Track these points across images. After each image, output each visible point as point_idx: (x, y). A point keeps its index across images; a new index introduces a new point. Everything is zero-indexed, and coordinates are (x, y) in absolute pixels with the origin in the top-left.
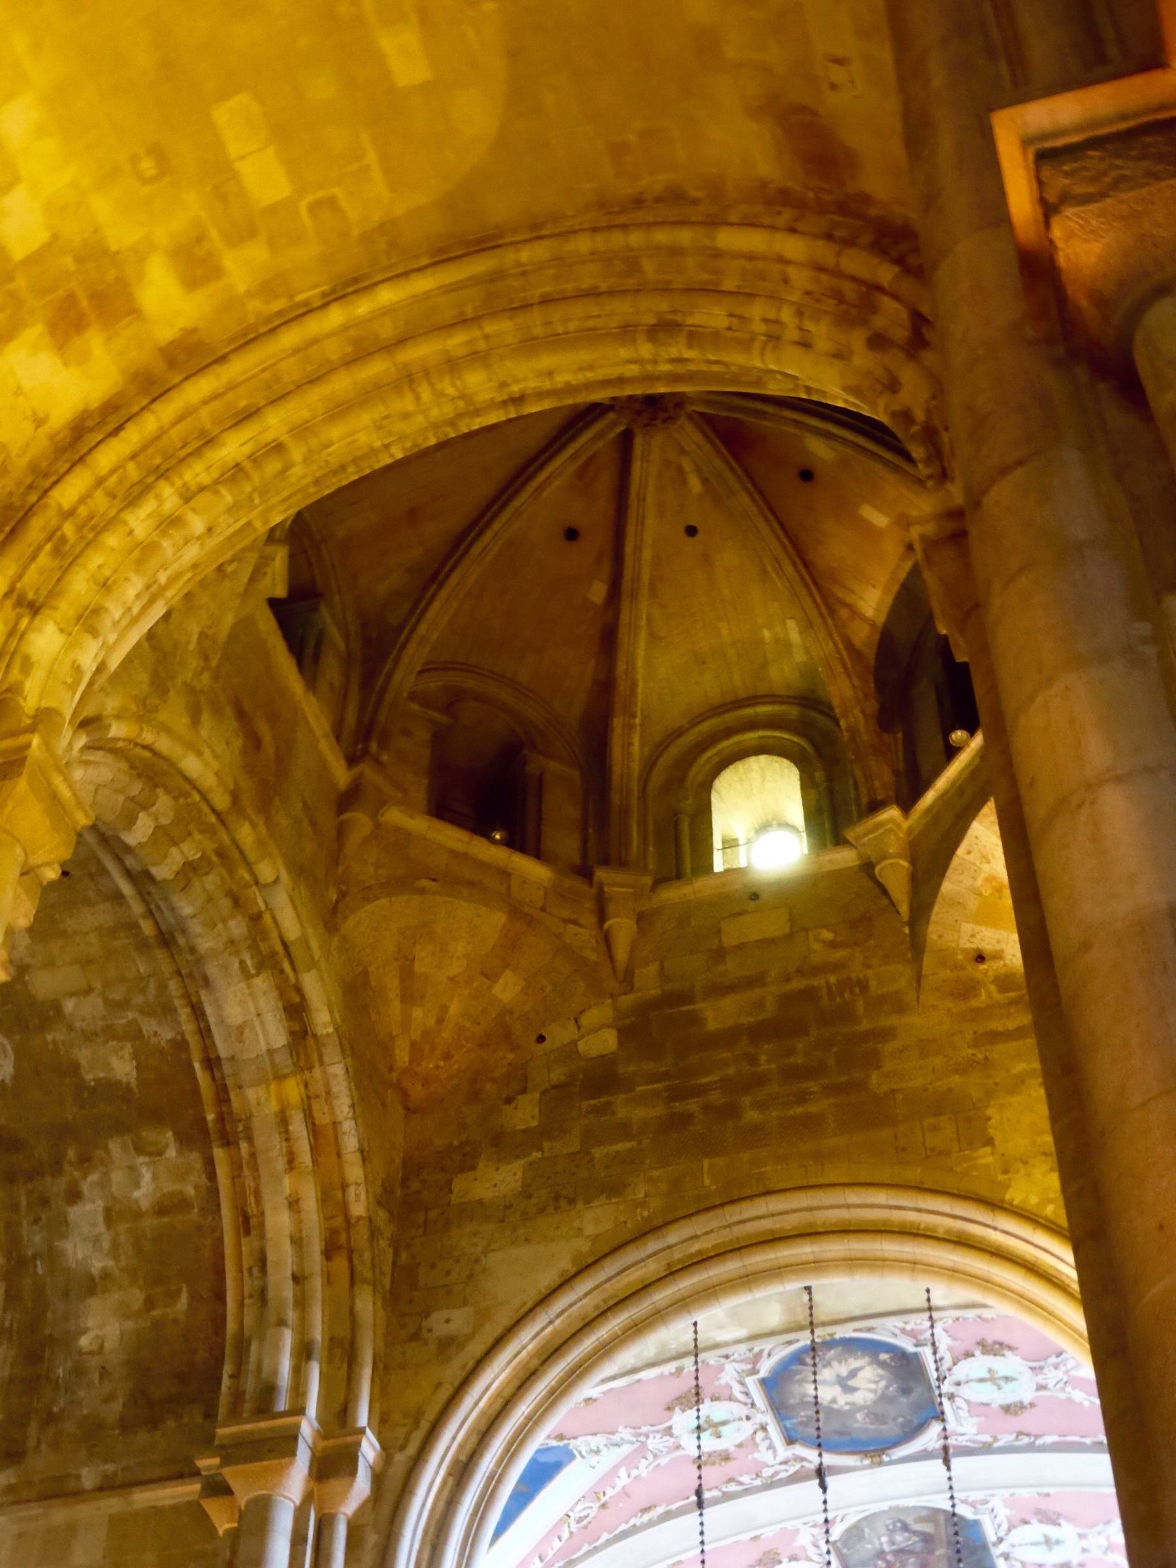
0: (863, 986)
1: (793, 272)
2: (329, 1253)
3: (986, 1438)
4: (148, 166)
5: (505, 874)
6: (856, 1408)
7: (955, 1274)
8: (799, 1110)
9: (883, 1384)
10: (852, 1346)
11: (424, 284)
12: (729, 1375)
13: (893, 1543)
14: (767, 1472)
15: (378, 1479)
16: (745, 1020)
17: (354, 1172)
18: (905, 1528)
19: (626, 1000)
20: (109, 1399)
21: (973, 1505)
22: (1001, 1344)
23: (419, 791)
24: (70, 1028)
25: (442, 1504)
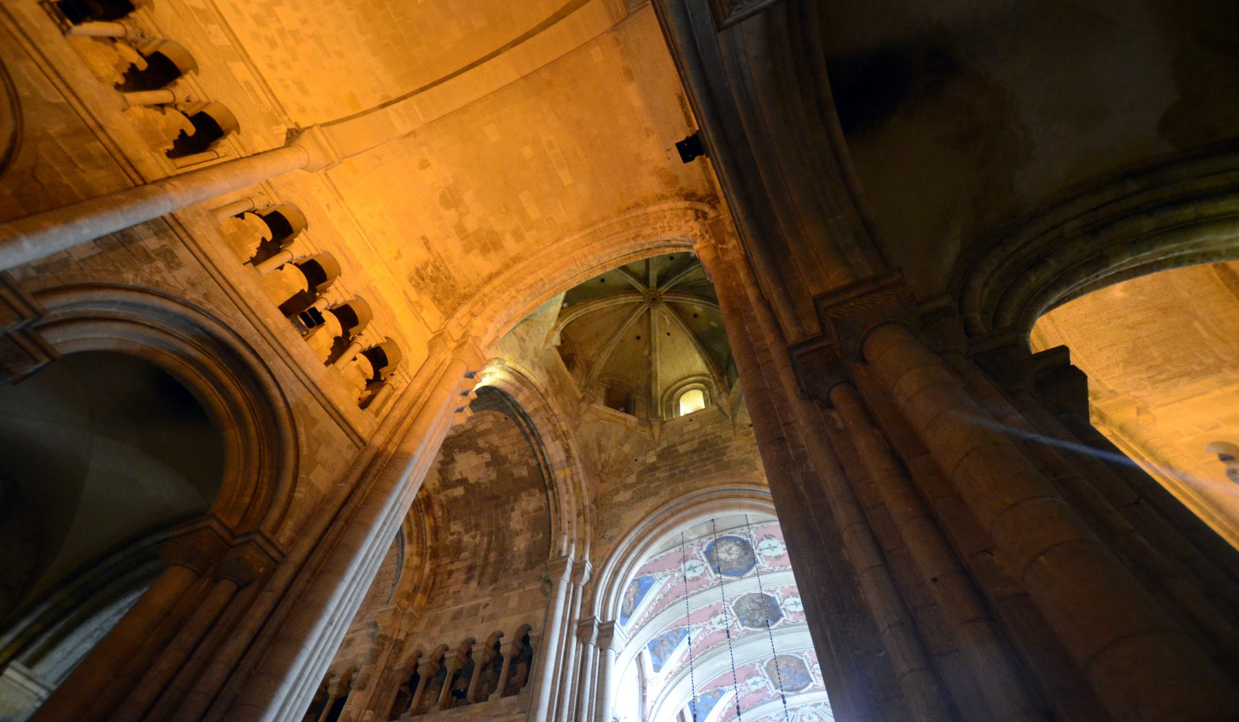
0: (720, 437)
1: (666, 213)
2: (578, 516)
3: (772, 568)
4: (503, 210)
5: (625, 419)
6: (733, 560)
7: (752, 507)
8: (704, 468)
9: (739, 551)
10: (728, 539)
11: (576, 236)
12: (695, 551)
13: (751, 607)
14: (710, 584)
15: (591, 576)
16: (689, 449)
17: (585, 493)
18: (753, 601)
19: (658, 449)
20: (521, 563)
21: (772, 592)
22: (771, 535)
23: (601, 401)
24: (511, 463)
25: (610, 583)
